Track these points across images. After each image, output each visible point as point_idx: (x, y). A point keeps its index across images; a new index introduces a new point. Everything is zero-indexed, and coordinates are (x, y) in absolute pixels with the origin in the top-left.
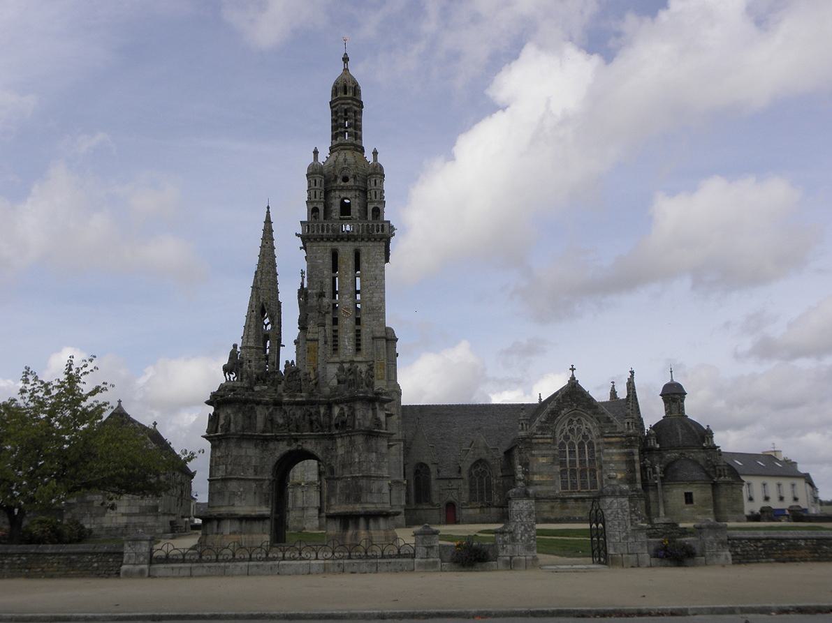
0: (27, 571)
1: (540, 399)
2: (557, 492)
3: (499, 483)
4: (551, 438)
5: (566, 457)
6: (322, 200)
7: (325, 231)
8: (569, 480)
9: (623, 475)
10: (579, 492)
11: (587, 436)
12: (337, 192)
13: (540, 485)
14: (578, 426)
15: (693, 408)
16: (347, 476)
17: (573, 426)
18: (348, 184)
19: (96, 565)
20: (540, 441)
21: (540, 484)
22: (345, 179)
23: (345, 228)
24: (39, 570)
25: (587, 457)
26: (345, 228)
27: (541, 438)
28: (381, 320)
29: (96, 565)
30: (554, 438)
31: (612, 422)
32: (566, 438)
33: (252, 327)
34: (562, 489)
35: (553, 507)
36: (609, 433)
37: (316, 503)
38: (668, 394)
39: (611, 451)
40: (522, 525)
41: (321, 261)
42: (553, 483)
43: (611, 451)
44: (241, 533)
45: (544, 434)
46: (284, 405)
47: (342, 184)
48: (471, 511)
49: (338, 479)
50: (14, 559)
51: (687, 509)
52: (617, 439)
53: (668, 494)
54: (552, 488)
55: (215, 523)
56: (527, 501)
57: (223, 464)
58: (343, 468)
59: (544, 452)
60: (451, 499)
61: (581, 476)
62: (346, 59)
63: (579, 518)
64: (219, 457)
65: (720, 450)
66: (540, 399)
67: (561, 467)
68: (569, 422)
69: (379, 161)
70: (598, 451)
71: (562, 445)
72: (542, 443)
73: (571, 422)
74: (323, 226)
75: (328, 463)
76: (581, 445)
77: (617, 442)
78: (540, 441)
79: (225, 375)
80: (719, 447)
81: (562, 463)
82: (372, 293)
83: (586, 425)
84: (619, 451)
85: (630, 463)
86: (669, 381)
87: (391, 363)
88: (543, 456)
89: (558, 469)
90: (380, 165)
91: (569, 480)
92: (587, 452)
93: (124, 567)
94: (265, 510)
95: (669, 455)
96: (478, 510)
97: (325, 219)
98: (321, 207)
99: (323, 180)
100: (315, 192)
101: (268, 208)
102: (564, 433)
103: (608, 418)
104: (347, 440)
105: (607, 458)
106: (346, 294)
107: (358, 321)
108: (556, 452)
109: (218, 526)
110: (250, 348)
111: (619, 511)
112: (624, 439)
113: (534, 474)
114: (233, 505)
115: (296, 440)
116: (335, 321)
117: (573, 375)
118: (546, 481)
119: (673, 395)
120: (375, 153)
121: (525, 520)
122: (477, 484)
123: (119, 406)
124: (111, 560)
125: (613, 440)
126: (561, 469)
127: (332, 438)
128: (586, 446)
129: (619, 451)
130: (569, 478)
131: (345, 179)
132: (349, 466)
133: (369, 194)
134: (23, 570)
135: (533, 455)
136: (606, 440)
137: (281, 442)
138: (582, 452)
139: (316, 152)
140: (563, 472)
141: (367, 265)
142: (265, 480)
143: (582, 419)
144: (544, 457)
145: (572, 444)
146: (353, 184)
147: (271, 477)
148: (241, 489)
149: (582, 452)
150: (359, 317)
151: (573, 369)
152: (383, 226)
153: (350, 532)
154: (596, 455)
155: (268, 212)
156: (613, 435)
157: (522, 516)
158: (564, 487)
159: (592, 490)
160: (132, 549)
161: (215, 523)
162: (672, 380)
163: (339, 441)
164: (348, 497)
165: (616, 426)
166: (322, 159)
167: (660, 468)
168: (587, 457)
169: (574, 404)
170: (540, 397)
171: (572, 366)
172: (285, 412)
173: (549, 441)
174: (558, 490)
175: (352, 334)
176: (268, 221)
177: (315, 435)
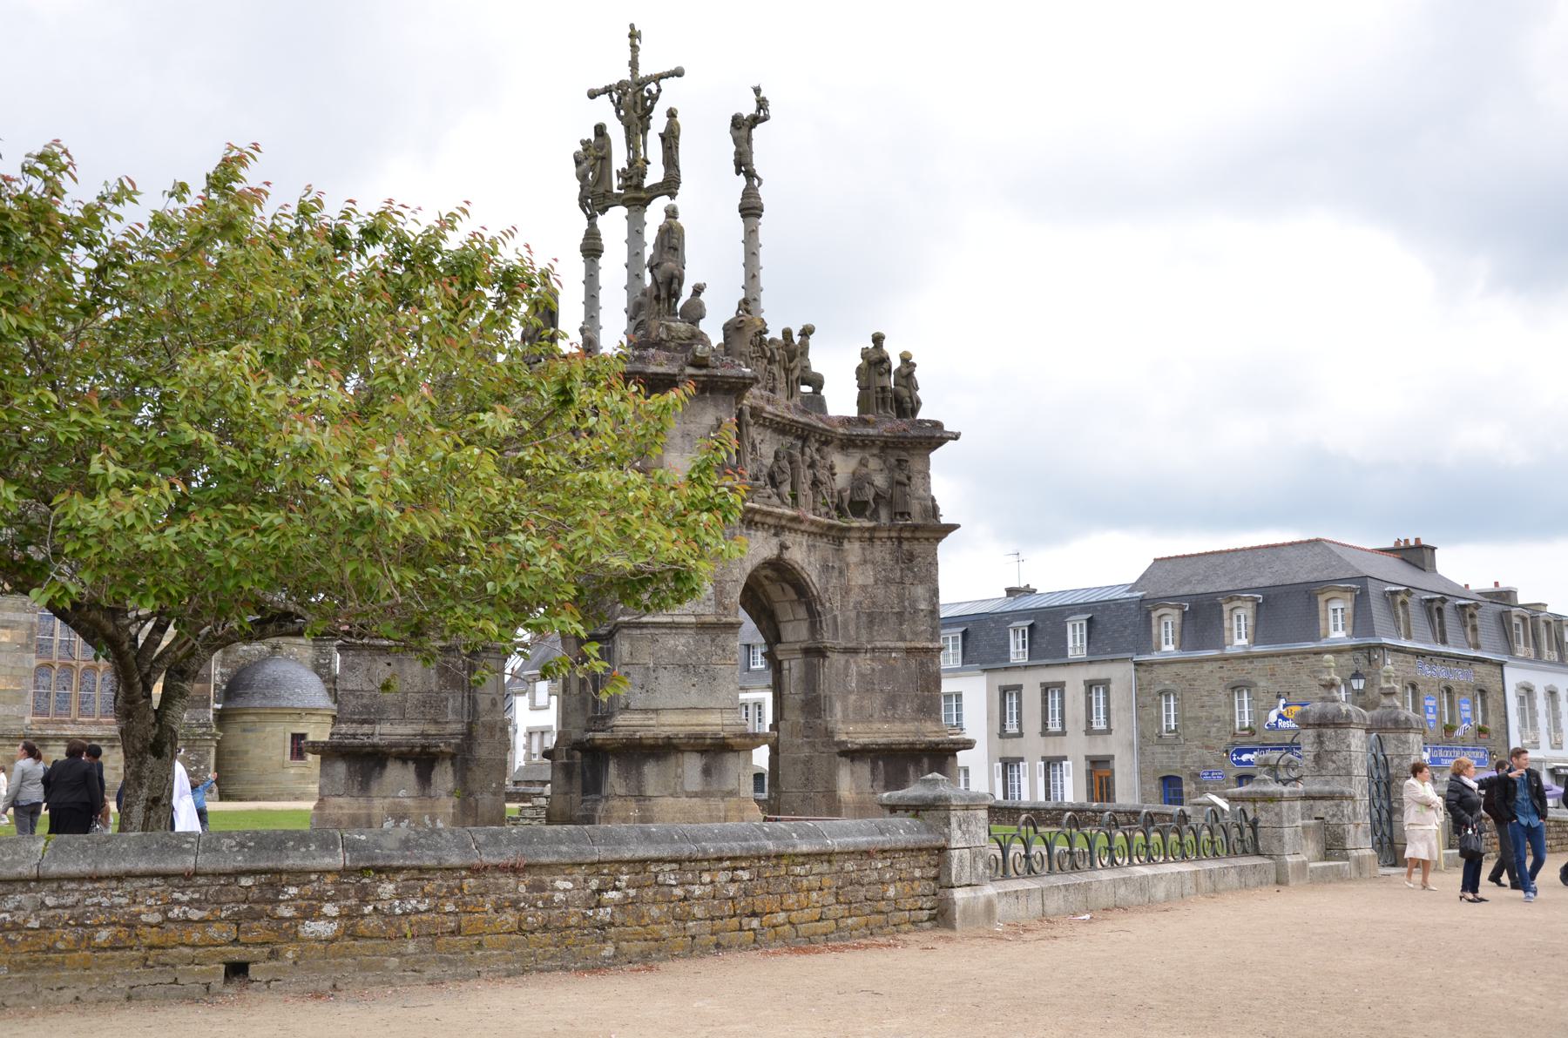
0: (755, 923)
5: (52, 635)
8: (53, 691)
10: (74, 722)
16: (891, 645)
42: (19, 697)
49: (854, 651)
51: (292, 771)
53: (250, 735)
54: (15, 710)
55: (691, 767)
58: (871, 622)
61: (82, 684)
109: (707, 772)
118: (5, 690)
126: (41, 661)
132: (893, 620)
134: (745, 921)
144: (6, 627)
164: (892, 702)
167: (222, 674)
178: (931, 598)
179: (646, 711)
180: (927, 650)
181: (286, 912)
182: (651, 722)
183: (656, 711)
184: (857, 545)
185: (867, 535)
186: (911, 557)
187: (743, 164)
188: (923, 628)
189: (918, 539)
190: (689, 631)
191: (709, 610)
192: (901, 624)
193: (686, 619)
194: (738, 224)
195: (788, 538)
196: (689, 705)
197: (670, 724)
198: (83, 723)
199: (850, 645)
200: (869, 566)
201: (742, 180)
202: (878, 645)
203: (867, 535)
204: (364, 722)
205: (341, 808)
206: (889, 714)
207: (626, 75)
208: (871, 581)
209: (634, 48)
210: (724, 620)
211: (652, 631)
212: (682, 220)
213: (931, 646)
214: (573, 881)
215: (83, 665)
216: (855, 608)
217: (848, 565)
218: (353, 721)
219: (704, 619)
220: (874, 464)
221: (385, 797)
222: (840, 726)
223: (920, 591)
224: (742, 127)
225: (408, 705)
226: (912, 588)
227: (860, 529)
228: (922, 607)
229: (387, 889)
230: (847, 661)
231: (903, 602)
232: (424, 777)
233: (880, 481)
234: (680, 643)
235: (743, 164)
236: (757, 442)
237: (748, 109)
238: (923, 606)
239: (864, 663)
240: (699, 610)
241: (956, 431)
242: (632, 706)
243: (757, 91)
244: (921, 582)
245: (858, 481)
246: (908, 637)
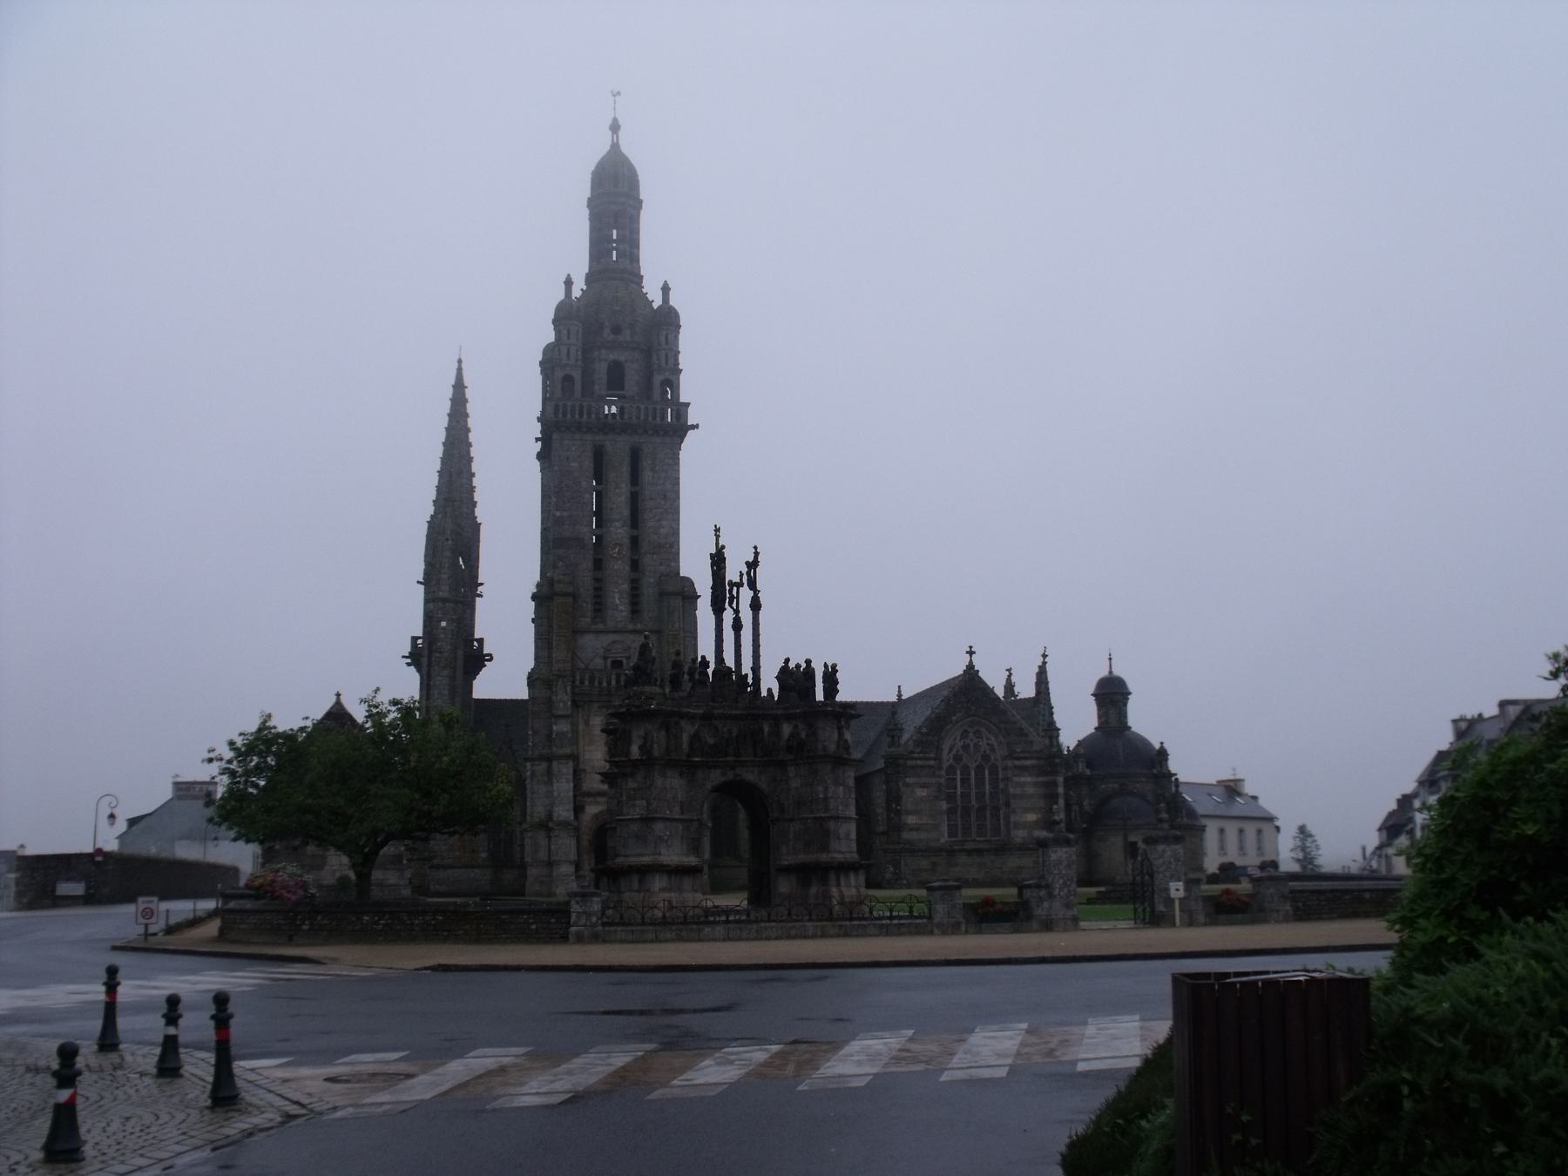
0: (445, 933)
1: (900, 695)
2: (942, 841)
4: (935, 759)
6: (580, 363)
7: (585, 416)
8: (959, 823)
9: (1039, 816)
10: (974, 841)
11: (987, 756)
12: (603, 352)
13: (917, 830)
14: (976, 740)
15: (1143, 720)
16: (806, 816)
17: (968, 741)
18: (621, 338)
19: (534, 927)
20: (919, 762)
21: (917, 828)
22: (617, 330)
23: (609, 410)
24: (461, 932)
25: (987, 787)
26: (609, 410)
27: (920, 759)
28: (673, 564)
29: (534, 927)
30: (938, 759)
31: (1026, 735)
32: (958, 758)
33: (447, 565)
34: (949, 837)
35: (934, 864)
36: (1022, 752)
37: (573, 856)
38: (1103, 694)
39: (1023, 779)
40: (1060, 878)
41: (575, 464)
43: (1023, 779)
44: (670, 890)
45: (925, 753)
46: (716, 719)
47: (611, 337)
49: (791, 820)
50: (428, 918)
52: (1033, 762)
55: (635, 878)
56: (1067, 849)
59: (925, 780)
62: (615, 127)
63: (974, 880)
64: (634, 789)
65: (1177, 779)
66: (900, 695)
67: (948, 803)
68: (962, 734)
69: (672, 302)
70: (1002, 780)
71: (951, 769)
72: (922, 767)
73: (965, 734)
74: (581, 407)
75: (776, 798)
76: (980, 769)
77: (1033, 767)
78: (919, 762)
80: (1176, 774)
81: (950, 798)
82: (659, 520)
83: (988, 739)
84: (1035, 780)
85: (1052, 798)
86: (1104, 673)
87: (688, 634)
88: (923, 786)
89: (944, 805)
90: (674, 309)
91: (959, 823)
92: (987, 780)
93: (573, 929)
94: (692, 860)
95: (1103, 786)
97: (583, 396)
98: (577, 375)
99: (580, 330)
100: (568, 350)
101: (460, 361)
102: (954, 752)
103: (1021, 729)
105: (1018, 791)
106: (618, 521)
107: (635, 565)
108: (943, 781)
109: (640, 881)
110: (444, 600)
111: (1172, 860)
112: (1042, 762)
113: (909, 813)
114: (659, 854)
116: (598, 564)
117: (971, 660)
119: (1111, 694)
120: (666, 289)
121: (1064, 872)
123: (338, 703)
124: (553, 920)
125: (1028, 763)
128: (987, 772)
129: (1035, 780)
130: (959, 819)
131: (617, 330)
133: (654, 357)
135: (908, 785)
136: (1017, 763)
137: (713, 771)
138: (980, 781)
139: (568, 283)
140: (951, 811)
141: (650, 474)
142: (693, 820)
143: (983, 730)
144: (924, 787)
145: (965, 769)
146: (628, 338)
148: (668, 833)
149: (980, 781)
150: (636, 557)
151: (971, 653)
152: (678, 411)
153: (813, 890)
154: (1001, 785)
155: (460, 370)
156: (1027, 755)
157: (1061, 867)
158: (952, 833)
159: (994, 839)
160: (581, 906)
161: (635, 878)
162: (1111, 672)
163: (792, 771)
165: (1032, 742)
166: (576, 293)
168: (987, 787)
169: (973, 708)
170: (899, 691)
171: (971, 647)
173: (932, 763)
174: (945, 839)
175: (626, 587)
176: (459, 387)
179: (625, 856)
181: (298, 922)
198: (979, 841)
207: (714, 552)
209: (717, 537)
213: (823, 815)
215: (976, 806)
220: (801, 726)
223: (820, 788)
224: (753, 565)
229: (319, 917)
233: (803, 735)
234: (634, 827)
237: (751, 559)
240: (642, 812)
243: (755, 548)
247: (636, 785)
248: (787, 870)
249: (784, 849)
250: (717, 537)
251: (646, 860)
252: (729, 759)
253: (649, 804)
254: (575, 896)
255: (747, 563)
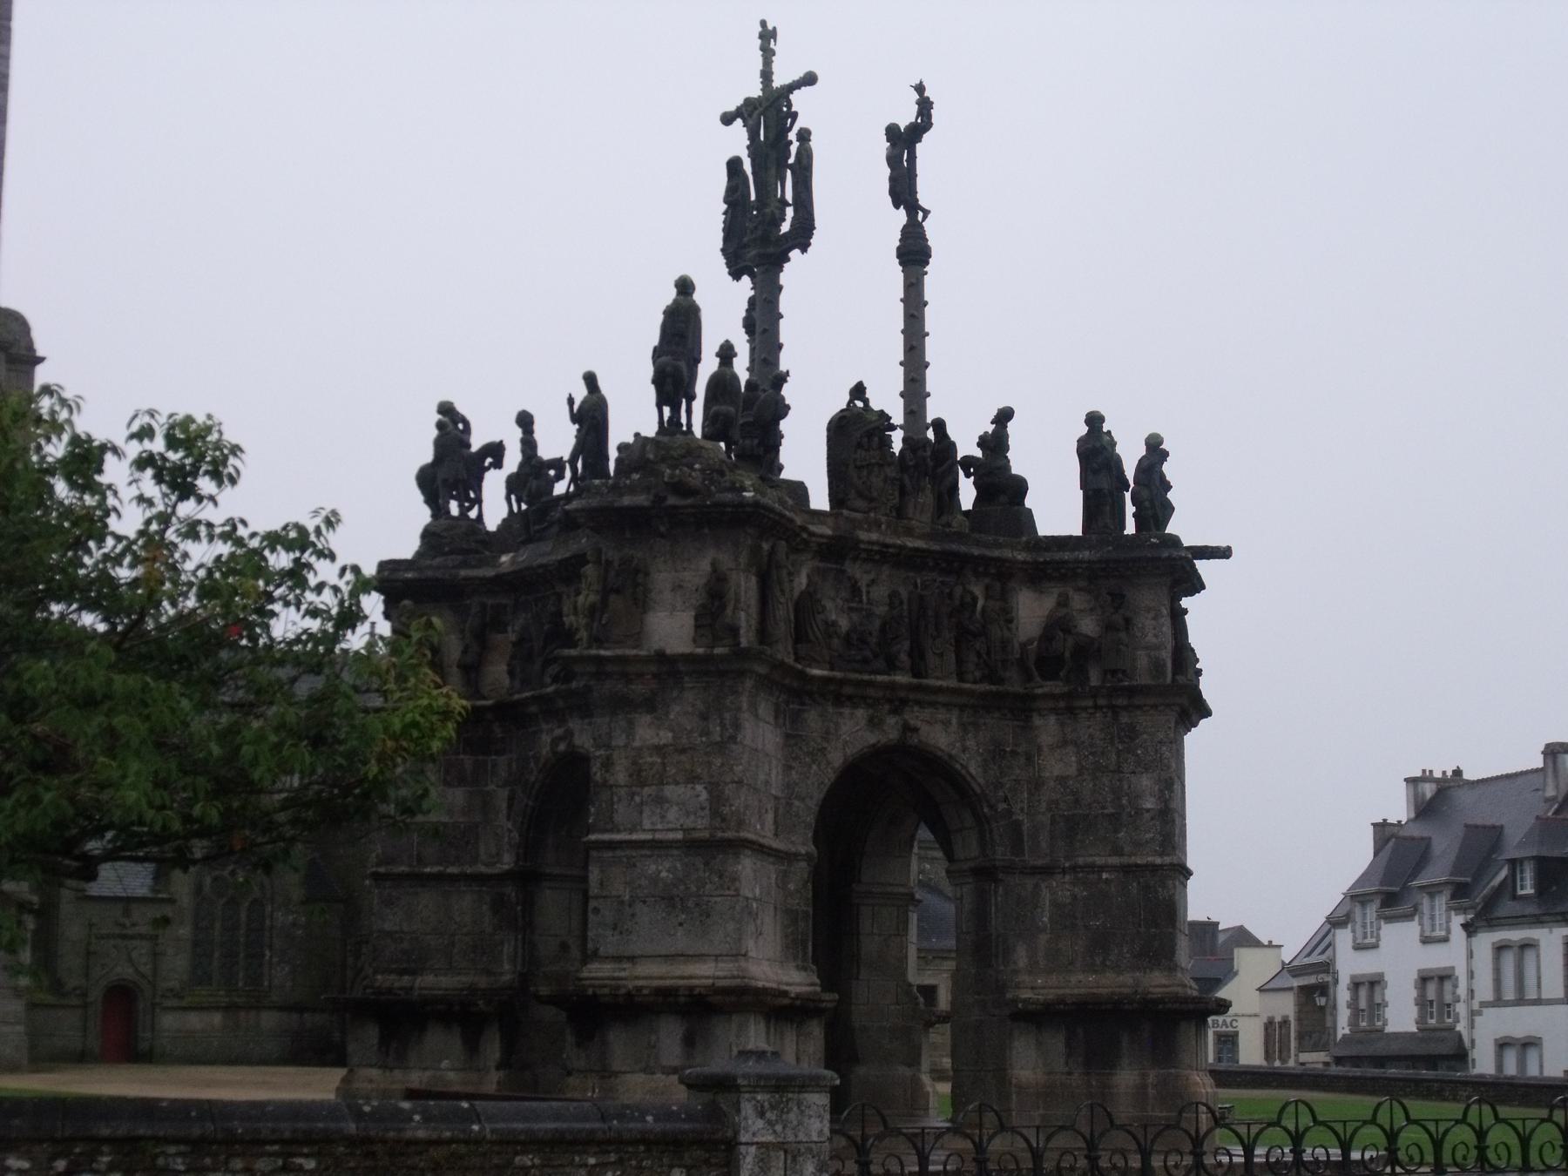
3: (294, 924)
16: (1099, 861)
48: (194, 1021)
49: (1047, 871)
57: (693, 779)
60: (124, 971)
64: (659, 749)
75: (1002, 806)
79: (659, 406)
94: (797, 980)
96: (217, 1018)
104: (1090, 728)
109: (689, 1041)
115: (899, 704)
122: (218, 925)
127: (1021, 709)
137: (847, 711)
147: (812, 848)
153: (1126, 1078)
160: (770, 1123)
163: (1047, 729)
172: (855, 590)
177: (971, 693)
178: (1161, 791)
179: (618, 959)
180: (1154, 868)
182: (623, 974)
183: (632, 959)
184: (1052, 719)
185: (1062, 704)
186: (1132, 732)
187: (903, 190)
188: (1148, 836)
189: (1139, 707)
190: (675, 852)
191: (700, 824)
192: (1116, 831)
193: (671, 836)
194: (895, 276)
195: (438, 735)
196: (673, 951)
197: (650, 974)
199: (1040, 862)
200: (1070, 749)
201: (901, 216)
202: (1081, 861)
203: (1062, 704)
204: (402, 972)
205: (371, 1081)
206: (1098, 960)
207: (756, 91)
208: (1072, 771)
209: (768, 54)
210: (720, 834)
211: (628, 852)
212: (697, 297)
213: (1158, 861)
214: (30, 1159)
216: (1049, 809)
217: (1040, 749)
218: (391, 972)
219: (696, 835)
220: (1078, 601)
221: (425, 1069)
222: (1025, 978)
223: (1146, 782)
225: (456, 951)
226: (1133, 778)
227: (1052, 696)
228: (1148, 806)
230: (1036, 886)
231: (1119, 799)
232: (472, 1045)
234: (663, 869)
235: (903, 190)
236: (863, 584)
237: (906, 116)
238: (1149, 804)
239: (1058, 890)
240: (689, 823)
241: (1223, 544)
242: (602, 951)
243: (920, 88)
244: (1147, 770)
245: (1058, 625)
246: (1127, 849)
247: (666, 737)
248: (1039, 1017)
249: (1021, 957)
250: (768, 54)
251: (704, 973)
252: (902, 678)
253: (717, 798)
254: (754, 1089)
255: (892, 132)
